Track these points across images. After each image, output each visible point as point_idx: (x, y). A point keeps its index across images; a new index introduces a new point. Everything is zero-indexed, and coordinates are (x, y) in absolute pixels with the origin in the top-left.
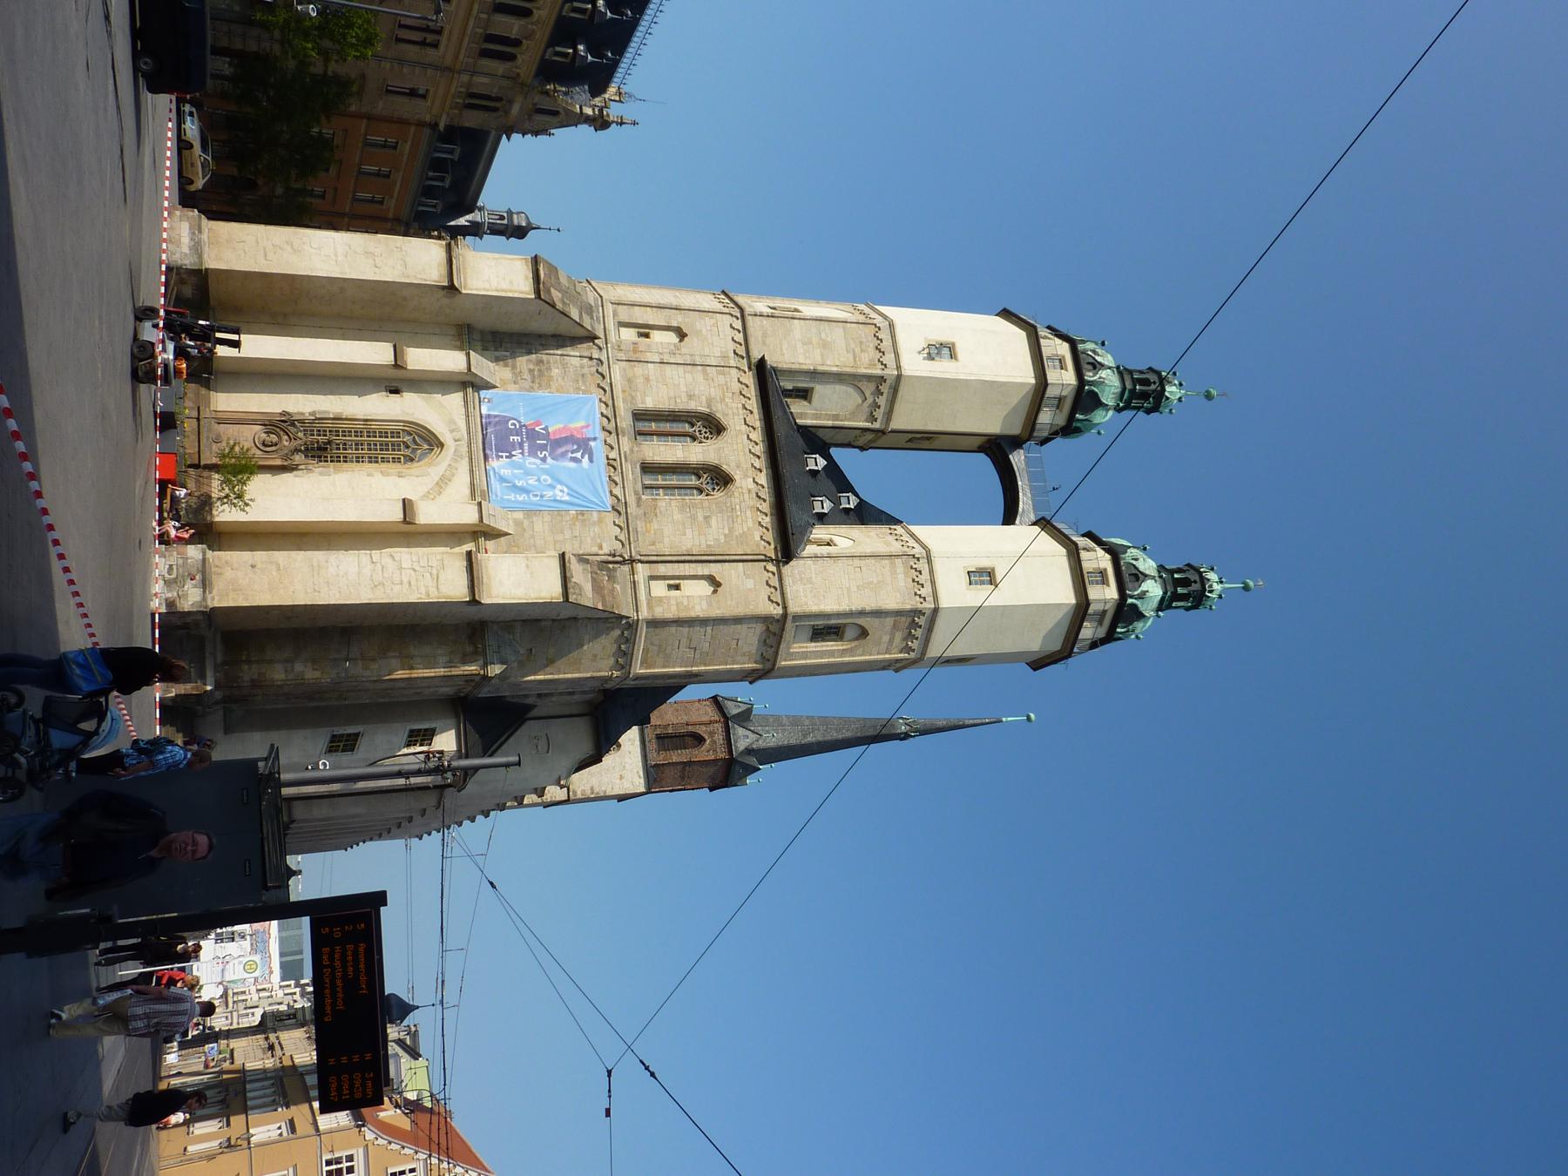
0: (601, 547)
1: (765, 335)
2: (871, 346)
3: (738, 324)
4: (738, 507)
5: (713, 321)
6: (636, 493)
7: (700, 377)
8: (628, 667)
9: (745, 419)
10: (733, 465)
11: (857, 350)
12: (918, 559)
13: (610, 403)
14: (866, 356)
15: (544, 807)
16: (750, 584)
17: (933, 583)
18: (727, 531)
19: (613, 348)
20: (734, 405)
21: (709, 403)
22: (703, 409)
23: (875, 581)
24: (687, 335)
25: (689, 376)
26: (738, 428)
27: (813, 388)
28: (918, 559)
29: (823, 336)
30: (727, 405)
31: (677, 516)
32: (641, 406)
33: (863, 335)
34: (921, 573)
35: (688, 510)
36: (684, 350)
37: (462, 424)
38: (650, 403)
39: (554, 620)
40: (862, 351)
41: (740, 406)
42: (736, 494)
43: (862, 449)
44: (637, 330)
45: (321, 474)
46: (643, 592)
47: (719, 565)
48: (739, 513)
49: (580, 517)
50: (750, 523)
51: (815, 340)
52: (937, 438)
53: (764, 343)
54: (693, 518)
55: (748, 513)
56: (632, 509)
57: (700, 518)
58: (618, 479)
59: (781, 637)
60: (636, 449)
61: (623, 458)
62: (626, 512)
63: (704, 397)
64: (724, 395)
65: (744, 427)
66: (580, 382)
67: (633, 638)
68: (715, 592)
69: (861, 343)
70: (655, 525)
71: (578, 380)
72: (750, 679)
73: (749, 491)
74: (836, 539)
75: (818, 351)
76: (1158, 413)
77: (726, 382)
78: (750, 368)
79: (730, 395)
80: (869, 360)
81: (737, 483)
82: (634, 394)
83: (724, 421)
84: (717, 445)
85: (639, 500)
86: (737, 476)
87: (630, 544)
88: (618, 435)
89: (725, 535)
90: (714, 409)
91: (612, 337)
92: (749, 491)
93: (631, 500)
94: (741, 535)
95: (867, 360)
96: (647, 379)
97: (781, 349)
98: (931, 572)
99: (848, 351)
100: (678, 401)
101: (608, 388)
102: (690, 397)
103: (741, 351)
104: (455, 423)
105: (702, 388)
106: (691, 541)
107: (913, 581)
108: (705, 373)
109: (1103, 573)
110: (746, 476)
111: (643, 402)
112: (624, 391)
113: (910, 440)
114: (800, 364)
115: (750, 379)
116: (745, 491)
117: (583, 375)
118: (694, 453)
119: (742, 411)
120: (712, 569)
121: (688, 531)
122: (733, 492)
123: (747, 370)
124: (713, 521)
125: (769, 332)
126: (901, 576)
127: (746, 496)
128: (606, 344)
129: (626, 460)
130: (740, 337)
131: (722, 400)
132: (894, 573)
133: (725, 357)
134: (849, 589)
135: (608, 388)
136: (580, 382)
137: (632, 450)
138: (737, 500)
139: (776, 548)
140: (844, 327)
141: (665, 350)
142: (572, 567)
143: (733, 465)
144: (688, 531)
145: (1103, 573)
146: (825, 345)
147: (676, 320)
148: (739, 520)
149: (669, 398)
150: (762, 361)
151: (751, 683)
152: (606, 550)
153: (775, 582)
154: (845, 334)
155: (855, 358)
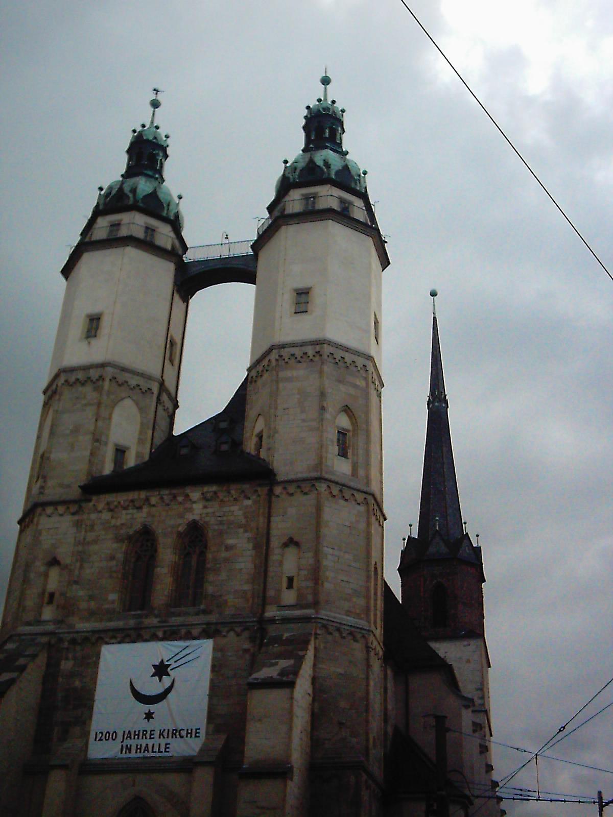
0: (246, 651)
1: (61, 485)
3: (49, 510)
4: (219, 519)
6: (197, 614)
7: (95, 548)
8: (364, 632)
10: (180, 521)
11: (84, 402)
13: (111, 634)
15: (490, 667)
16: (292, 511)
17: (303, 344)
18: (241, 530)
19: (59, 628)
23: (298, 396)
26: (145, 515)
27: (116, 445)
28: (281, 356)
30: (122, 524)
31: (223, 575)
35: (218, 566)
37: (117, 778)
38: (113, 597)
39: (314, 700)
41: (124, 512)
42: (207, 519)
43: (176, 406)
44: (45, 605)
46: (296, 612)
48: (225, 518)
50: (235, 508)
52: (172, 337)
54: (226, 560)
56: (213, 618)
58: (183, 631)
59: (343, 485)
60: (156, 612)
61: (164, 624)
63: (115, 545)
65: (145, 510)
66: (90, 661)
67: (336, 625)
68: (297, 544)
72: (382, 520)
73: (205, 507)
74: (257, 430)
76: (168, 148)
78: (90, 501)
81: (197, 517)
85: (205, 612)
86: (190, 517)
87: (245, 622)
88: (141, 628)
89: (246, 531)
91: (50, 627)
92: (205, 507)
93: (204, 619)
94: (246, 517)
98: (293, 345)
100: (114, 569)
101: (97, 636)
103: (73, 508)
106: (245, 562)
107: (300, 362)
108: (89, 544)
109: (306, 198)
110: (191, 510)
111: (113, 602)
112: (101, 620)
113: (171, 361)
116: (206, 511)
118: (167, 555)
119: (131, 511)
120: (275, 543)
121: (238, 566)
122: (204, 522)
123: (91, 504)
124: (230, 542)
126: (294, 373)
127: (210, 510)
129: (165, 622)
130: (61, 509)
132: (289, 380)
134: (304, 421)
135: (97, 636)
136: (90, 661)
142: (262, 677)
143: (180, 521)
144: (238, 566)
145: (306, 198)
146: (76, 430)
147: (40, 566)
148: (232, 518)
149: (111, 577)
151: (385, 519)
152: (246, 646)
153: (292, 489)
155: (89, 404)
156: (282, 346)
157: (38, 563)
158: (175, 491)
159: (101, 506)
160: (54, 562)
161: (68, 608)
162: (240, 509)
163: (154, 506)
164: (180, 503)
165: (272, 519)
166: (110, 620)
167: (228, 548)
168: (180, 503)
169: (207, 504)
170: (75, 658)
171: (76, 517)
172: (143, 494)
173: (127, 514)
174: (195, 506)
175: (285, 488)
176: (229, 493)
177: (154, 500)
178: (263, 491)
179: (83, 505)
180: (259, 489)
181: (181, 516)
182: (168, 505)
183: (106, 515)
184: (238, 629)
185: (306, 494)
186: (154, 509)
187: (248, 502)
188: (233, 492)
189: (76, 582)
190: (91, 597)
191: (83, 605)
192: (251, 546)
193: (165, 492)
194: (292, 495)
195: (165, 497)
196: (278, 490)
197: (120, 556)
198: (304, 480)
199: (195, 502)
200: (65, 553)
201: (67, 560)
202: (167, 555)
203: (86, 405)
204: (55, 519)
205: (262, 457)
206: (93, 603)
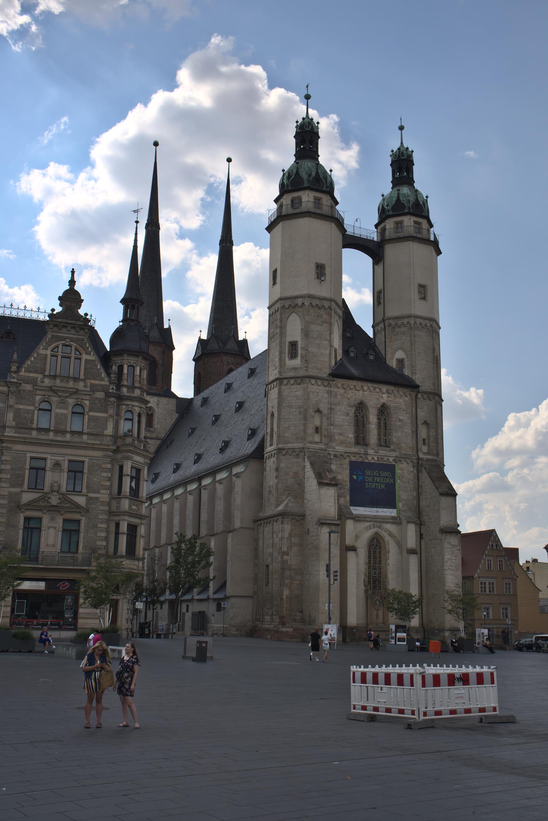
0: (412, 471)
2: (319, 311)
3: (313, 381)
5: (311, 393)
7: (338, 407)
9: (357, 390)
12: (415, 322)
13: (353, 455)
14: (324, 316)
18: (405, 413)
20: (351, 394)
21: (349, 406)
22: (353, 410)
24: (318, 409)
25: (339, 413)
26: (361, 395)
29: (315, 336)
31: (399, 434)
32: (353, 440)
33: (314, 314)
34: (421, 323)
36: (326, 412)
38: (351, 435)
40: (322, 317)
41: (351, 391)
42: (389, 404)
45: (389, 584)
47: (418, 420)
49: (401, 478)
50: (401, 400)
51: (318, 342)
53: (320, 370)
55: (397, 400)
57: (399, 423)
58: (386, 459)
62: (399, 457)
63: (348, 408)
64: (346, 398)
65: (361, 392)
69: (318, 316)
70: (403, 445)
71: (343, 468)
73: (388, 397)
75: (323, 342)
77: (340, 395)
78: (334, 381)
79: (346, 394)
80: (326, 315)
82: (347, 442)
83: (359, 401)
84: (369, 407)
86: (383, 401)
87: (412, 458)
89: (406, 414)
90: (353, 404)
92: (388, 397)
95: (326, 316)
96: (341, 434)
97: (323, 361)
99: (322, 325)
102: (347, 414)
103: (326, 383)
104: (367, 527)
105: (343, 408)
106: (408, 430)
107: (423, 328)
110: (382, 397)
111: (351, 438)
112: (347, 447)
114: (330, 353)
115: (340, 382)
116: (388, 399)
117: (341, 465)
118: (373, 418)
119: (354, 391)
120: (419, 423)
121: (406, 430)
123: (335, 383)
124: (401, 417)
125: (315, 365)
127: (390, 399)
128: (327, 450)
130: (319, 382)
131: (349, 399)
133: (330, 393)
137: (373, 449)
138: (392, 404)
139: (412, 391)
140: (310, 323)
141: (327, 422)
148: (400, 405)
149: (349, 425)
150: (330, 375)
152: (412, 469)
154: (313, 324)
155: (325, 322)
156: (416, 317)
157: (311, 410)
158: (374, 385)
159: (340, 385)
160: (318, 411)
161: (330, 438)
162: (403, 402)
163: (365, 391)
164: (377, 392)
165: (418, 410)
166: (351, 447)
167: (400, 420)
168: (377, 392)
169: (390, 395)
170: (337, 464)
171: (327, 388)
172: (360, 383)
173: (352, 392)
174: (384, 395)
175: (422, 395)
176: (398, 392)
177: (365, 388)
178: (414, 394)
179: (331, 382)
180: (411, 393)
181: (378, 400)
182: (372, 392)
183: (341, 391)
184: (408, 461)
185: (431, 400)
186: (365, 393)
187: (407, 399)
188: (400, 392)
189: (332, 425)
190: (341, 434)
191: (337, 437)
192: (409, 421)
193: (370, 385)
194: (425, 399)
195: (370, 387)
196: (419, 396)
197: (352, 414)
198: (431, 393)
199: (384, 393)
200: (323, 406)
201: (325, 412)
202: (373, 418)
203: (322, 322)
204: (315, 387)
205: (406, 374)
206: (341, 437)
